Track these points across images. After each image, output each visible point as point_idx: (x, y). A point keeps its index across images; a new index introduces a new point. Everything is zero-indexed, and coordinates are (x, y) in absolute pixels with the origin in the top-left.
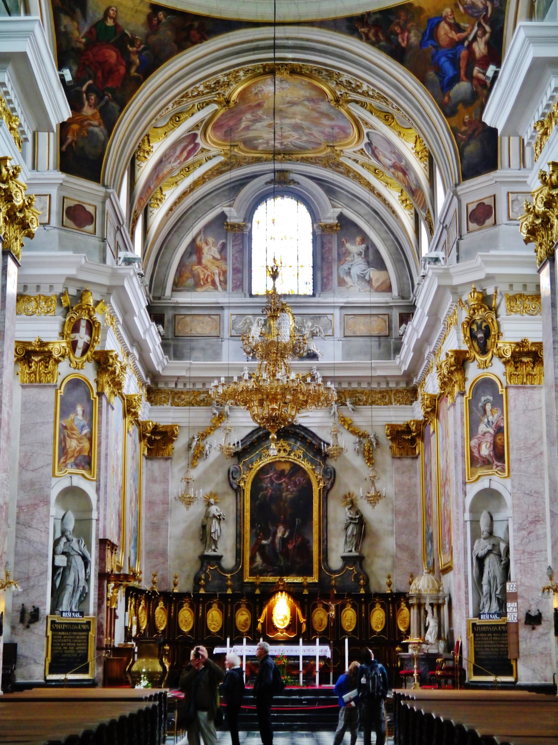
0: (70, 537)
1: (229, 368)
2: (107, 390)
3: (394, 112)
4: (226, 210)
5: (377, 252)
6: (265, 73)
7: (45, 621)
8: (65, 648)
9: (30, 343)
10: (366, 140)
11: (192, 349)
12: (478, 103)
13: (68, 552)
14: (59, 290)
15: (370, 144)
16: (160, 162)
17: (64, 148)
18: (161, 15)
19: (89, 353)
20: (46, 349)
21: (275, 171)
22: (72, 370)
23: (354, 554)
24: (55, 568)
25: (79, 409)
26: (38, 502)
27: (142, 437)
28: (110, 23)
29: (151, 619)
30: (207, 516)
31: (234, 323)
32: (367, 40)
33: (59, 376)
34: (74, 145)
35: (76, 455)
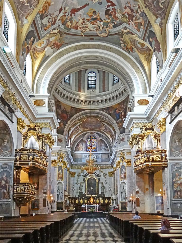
1: (84, 163)
3: (109, 123)
4: (83, 138)
5: (107, 145)
6: (89, 117)
10: (105, 127)
11: (78, 160)
12: (122, 122)
15: (105, 128)
16: (73, 131)
18: (73, 108)
21: (91, 132)
23: (103, 191)
27: (70, 174)
28: (65, 110)
29: (72, 201)
30: (80, 186)
31: (84, 156)
32: (105, 112)
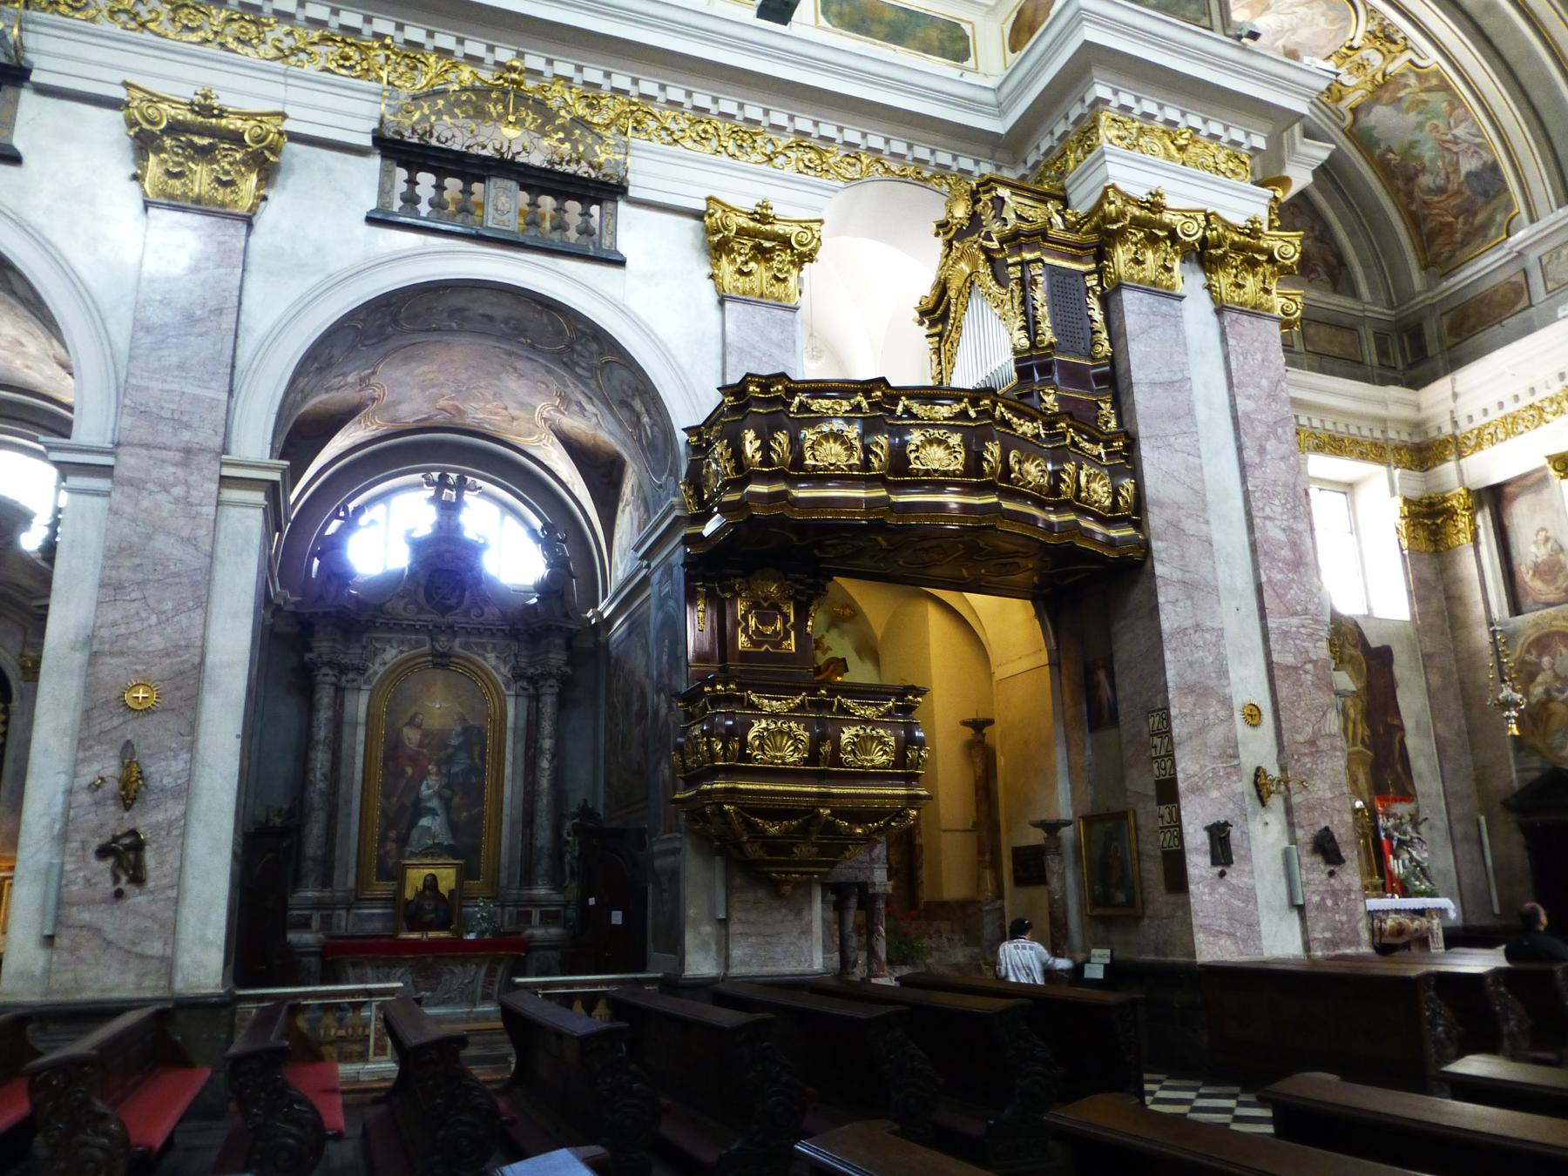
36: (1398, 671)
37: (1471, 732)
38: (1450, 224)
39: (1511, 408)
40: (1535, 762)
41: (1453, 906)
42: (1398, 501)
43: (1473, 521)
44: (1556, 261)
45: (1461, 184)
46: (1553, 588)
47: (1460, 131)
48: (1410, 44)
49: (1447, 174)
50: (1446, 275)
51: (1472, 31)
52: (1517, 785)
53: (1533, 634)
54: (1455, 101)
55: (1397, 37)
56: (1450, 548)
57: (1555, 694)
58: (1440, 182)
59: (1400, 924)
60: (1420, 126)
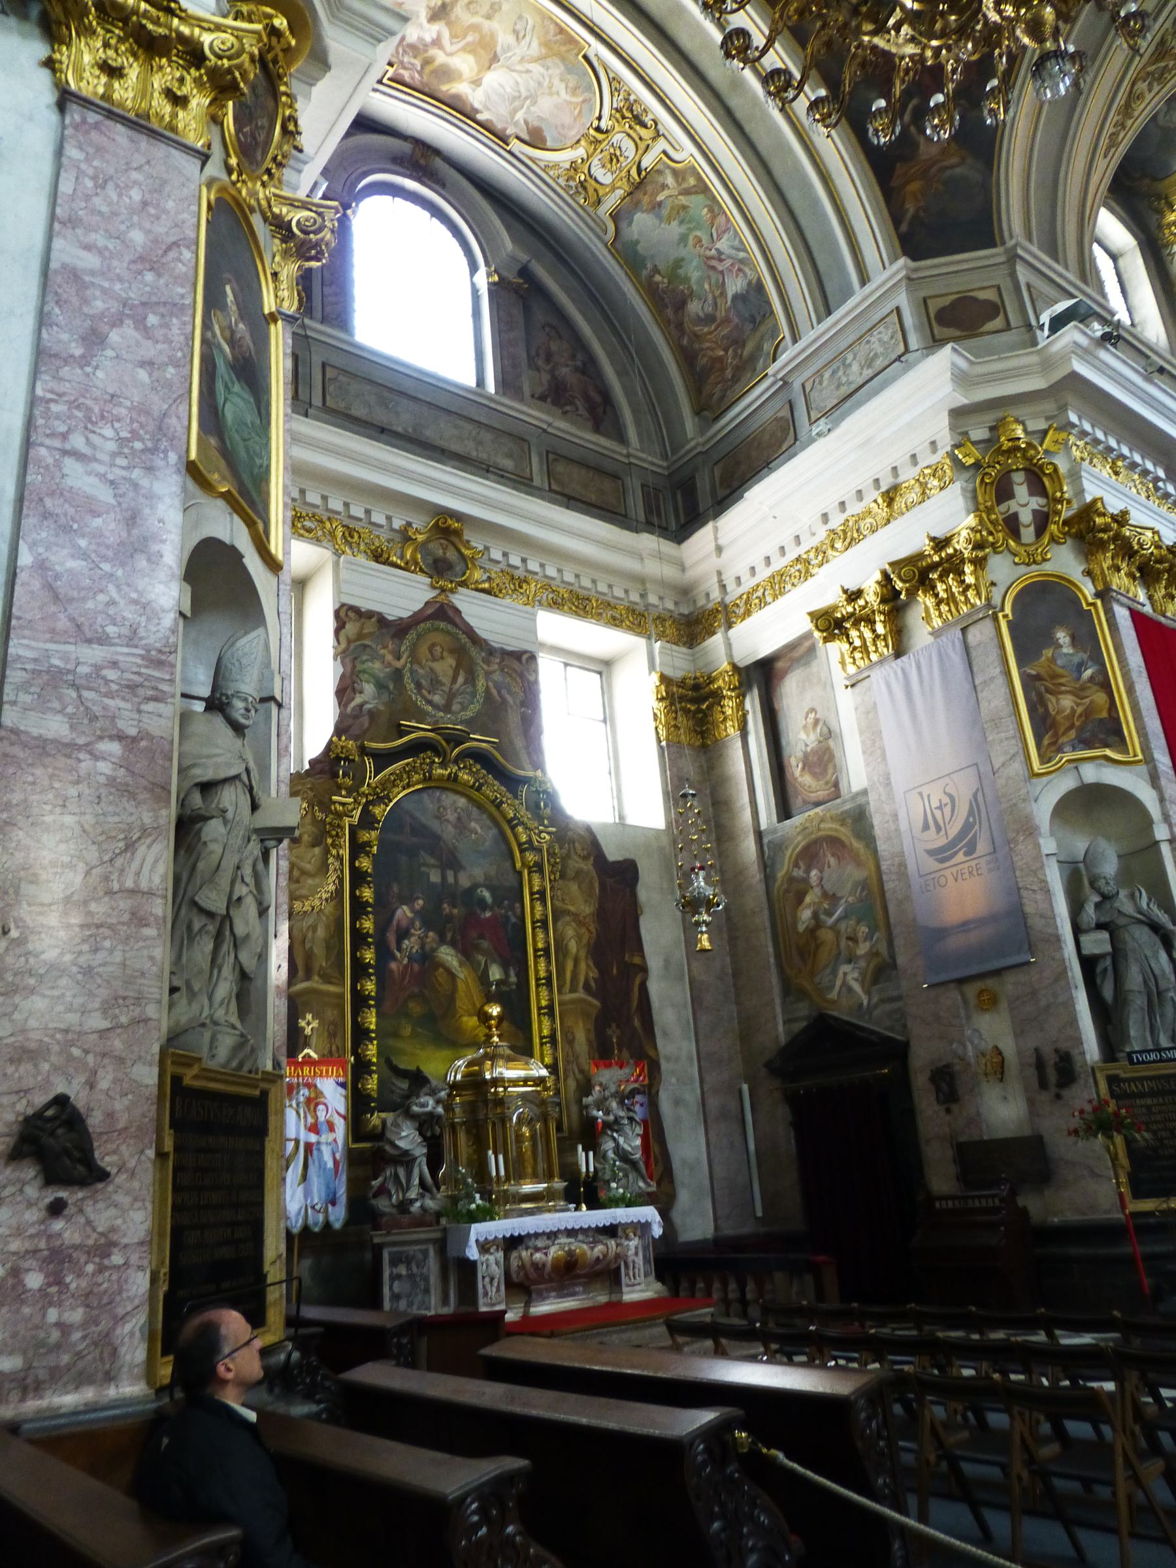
0: (1109, 889)
2: (1120, 581)
7: (1091, 1080)
8: (1164, 1134)
9: (920, 556)
13: (1112, 922)
14: (946, 440)
17: (904, 227)
19: (1053, 527)
20: (950, 551)
22: (1023, 569)
24: (1088, 964)
25: (1062, 636)
26: (1011, 835)
33: (994, 589)
34: (922, 214)
35: (1077, 723)
36: (643, 894)
37: (736, 974)
38: (720, 359)
39: (778, 564)
40: (803, 1010)
41: (658, 1218)
42: (655, 678)
43: (740, 706)
44: (819, 387)
45: (728, 311)
46: (822, 782)
47: (723, 245)
48: (662, 130)
49: (715, 298)
50: (717, 418)
51: (721, 112)
52: (783, 1040)
53: (800, 842)
54: (715, 207)
55: (648, 120)
56: (717, 740)
57: (823, 917)
58: (709, 309)
59: (570, 1253)
60: (683, 239)
